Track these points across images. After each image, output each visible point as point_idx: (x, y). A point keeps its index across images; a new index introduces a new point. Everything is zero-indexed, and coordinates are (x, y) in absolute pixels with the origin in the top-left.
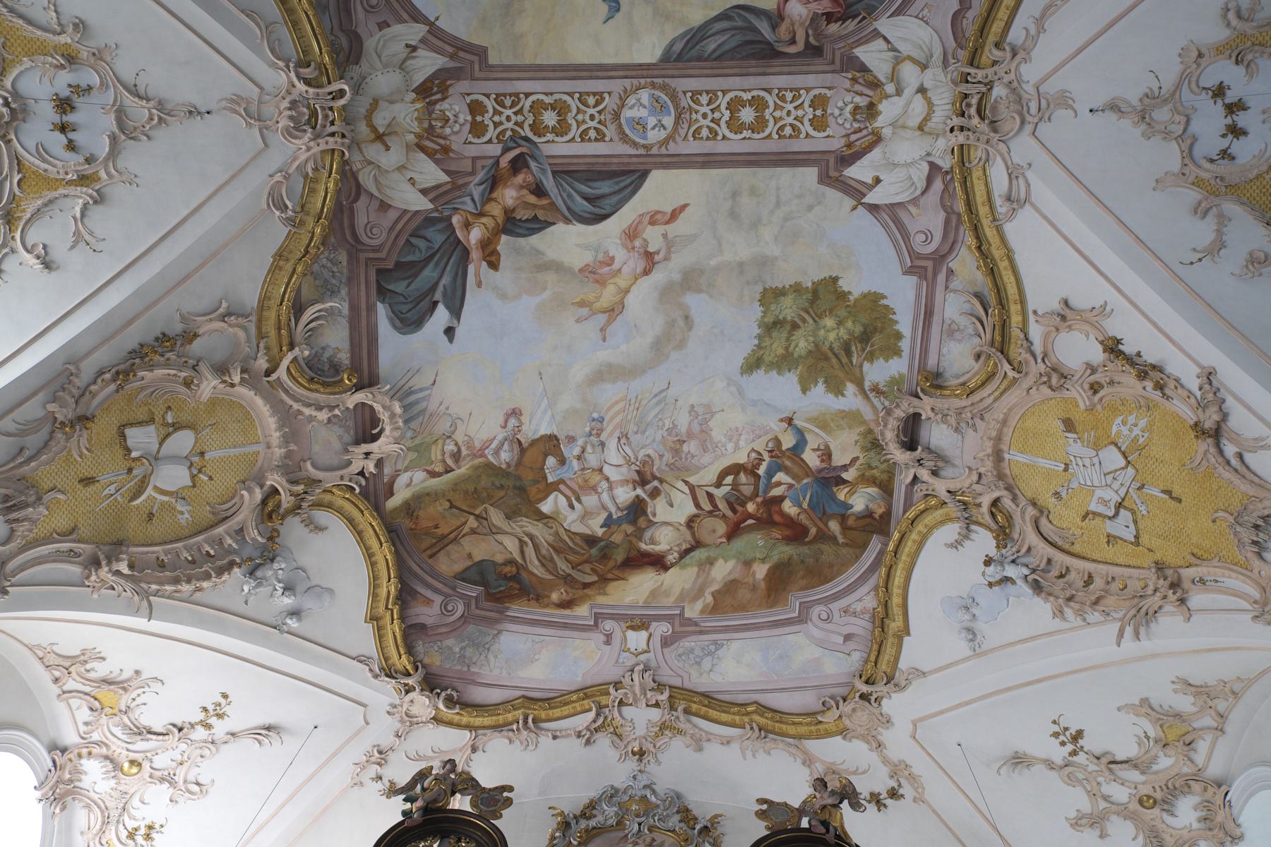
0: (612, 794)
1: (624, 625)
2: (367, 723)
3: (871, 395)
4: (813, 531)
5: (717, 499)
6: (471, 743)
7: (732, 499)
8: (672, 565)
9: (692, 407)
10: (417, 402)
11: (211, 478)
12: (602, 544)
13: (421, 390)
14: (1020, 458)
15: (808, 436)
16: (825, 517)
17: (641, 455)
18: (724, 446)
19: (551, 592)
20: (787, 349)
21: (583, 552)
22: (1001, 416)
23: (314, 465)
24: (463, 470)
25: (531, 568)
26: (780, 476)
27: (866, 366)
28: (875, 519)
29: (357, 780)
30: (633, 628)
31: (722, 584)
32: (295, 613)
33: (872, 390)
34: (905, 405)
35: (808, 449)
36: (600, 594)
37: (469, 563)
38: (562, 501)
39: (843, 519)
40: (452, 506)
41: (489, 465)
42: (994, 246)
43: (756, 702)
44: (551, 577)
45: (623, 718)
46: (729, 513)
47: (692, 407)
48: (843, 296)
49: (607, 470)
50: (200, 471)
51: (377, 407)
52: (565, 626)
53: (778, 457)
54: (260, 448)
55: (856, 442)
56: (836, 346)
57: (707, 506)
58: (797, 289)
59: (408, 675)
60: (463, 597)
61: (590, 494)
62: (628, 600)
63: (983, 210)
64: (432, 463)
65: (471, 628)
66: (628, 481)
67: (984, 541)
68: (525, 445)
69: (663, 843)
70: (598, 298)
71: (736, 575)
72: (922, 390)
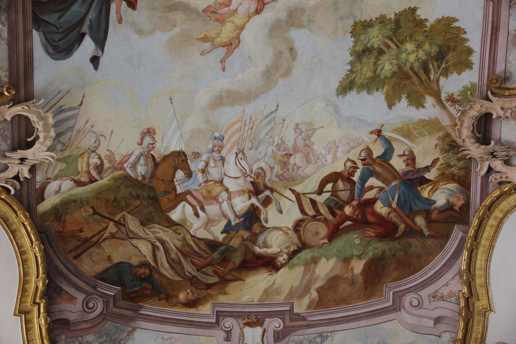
1: (242, 322)
3: (448, 105)
4: (402, 227)
5: (319, 204)
7: (332, 205)
8: (283, 266)
9: (297, 125)
12: (223, 248)
13: (71, 109)
15: (395, 145)
16: (412, 214)
17: (255, 168)
18: (324, 157)
19: (179, 292)
20: (375, 72)
21: (206, 255)
24: (104, 181)
26: (372, 181)
27: (442, 80)
28: (456, 211)
30: (250, 325)
31: (325, 281)
33: (448, 100)
36: (221, 294)
37: (108, 265)
38: (189, 210)
39: (427, 214)
40: (95, 213)
41: (127, 177)
44: (178, 278)
46: (330, 217)
47: (297, 125)
48: (420, 23)
49: (227, 182)
52: (191, 324)
53: (370, 164)
55: (436, 146)
56: (416, 66)
57: (311, 212)
58: (382, 20)
61: (211, 204)
62: (245, 298)
64: (78, 173)
65: (109, 325)
66: (244, 191)
68: (158, 160)
70: (218, 34)
71: (337, 272)
72: (492, 93)
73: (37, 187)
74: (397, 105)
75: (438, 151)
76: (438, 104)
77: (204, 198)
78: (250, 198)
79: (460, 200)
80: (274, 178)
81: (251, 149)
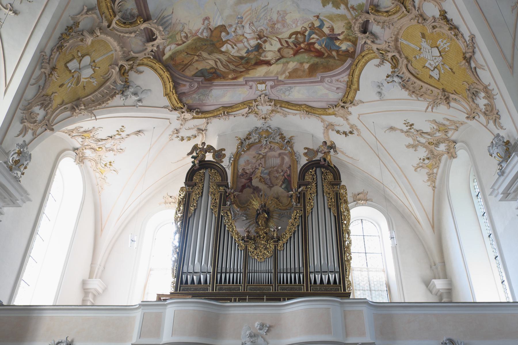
0: (257, 129)
1: (256, 83)
2: (171, 123)
3: (351, 10)
4: (326, 54)
6: (206, 122)
7: (295, 43)
8: (273, 64)
9: (278, 11)
10: (167, 21)
11: (99, 68)
12: (246, 58)
13: (168, 16)
14: (405, 42)
16: (331, 50)
17: (259, 29)
21: (239, 62)
22: (399, 27)
23: (134, 52)
24: (190, 41)
25: (220, 69)
26: (314, 36)
28: (350, 53)
29: (171, 139)
30: (259, 83)
32: (140, 100)
33: (351, 8)
35: (325, 27)
36: (246, 74)
39: (337, 52)
40: (188, 54)
43: (305, 104)
44: (228, 71)
45: (258, 109)
46: (294, 47)
47: (278, 11)
49: (246, 35)
50: (95, 67)
51: (153, 29)
52: (235, 85)
54: (113, 52)
55: (344, 26)
57: (286, 45)
59: (182, 108)
60: (196, 81)
62: (257, 75)
64: (177, 41)
65: (201, 90)
67: (387, 68)
68: (212, 29)
69: (274, 147)
73: (161, 50)
74: (327, 6)
75: (344, 28)
76: (346, 9)
77: (236, 41)
78: (257, 40)
79: (352, 49)
80: (268, 33)
81: (256, 22)
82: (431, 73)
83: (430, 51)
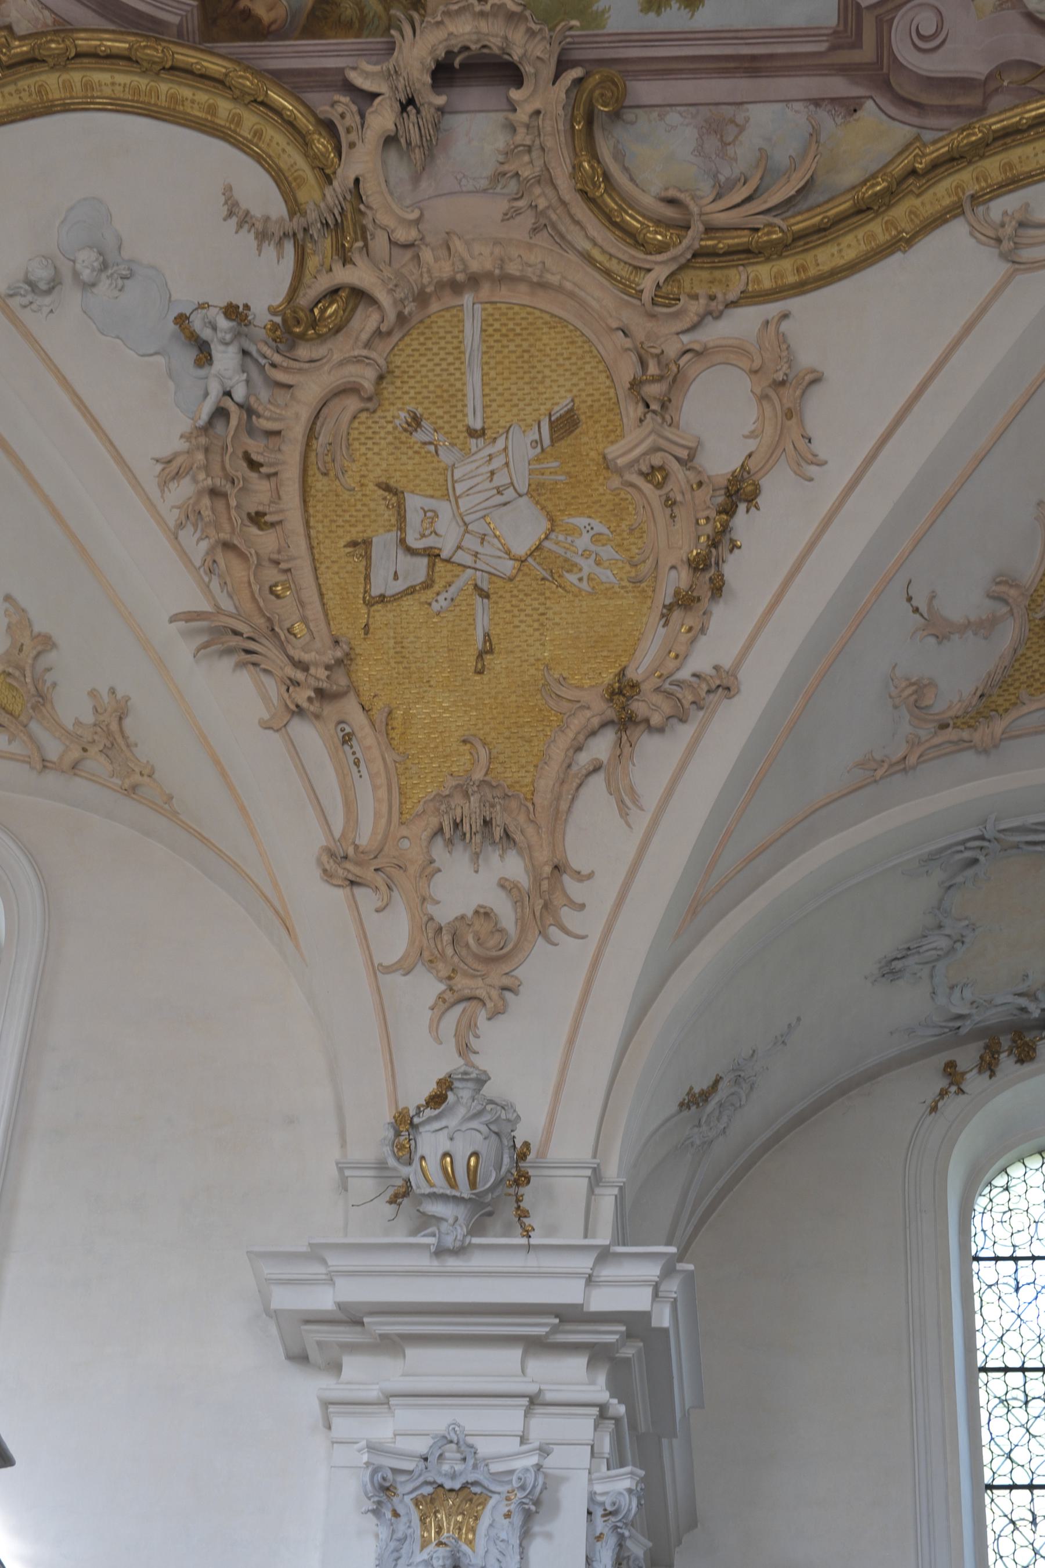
22: (554, 279)
34: (538, 49)
42: (917, 202)
63: (992, 167)
72: (578, 82)
79: (271, 9)
82: (383, 543)
83: (509, 493)
